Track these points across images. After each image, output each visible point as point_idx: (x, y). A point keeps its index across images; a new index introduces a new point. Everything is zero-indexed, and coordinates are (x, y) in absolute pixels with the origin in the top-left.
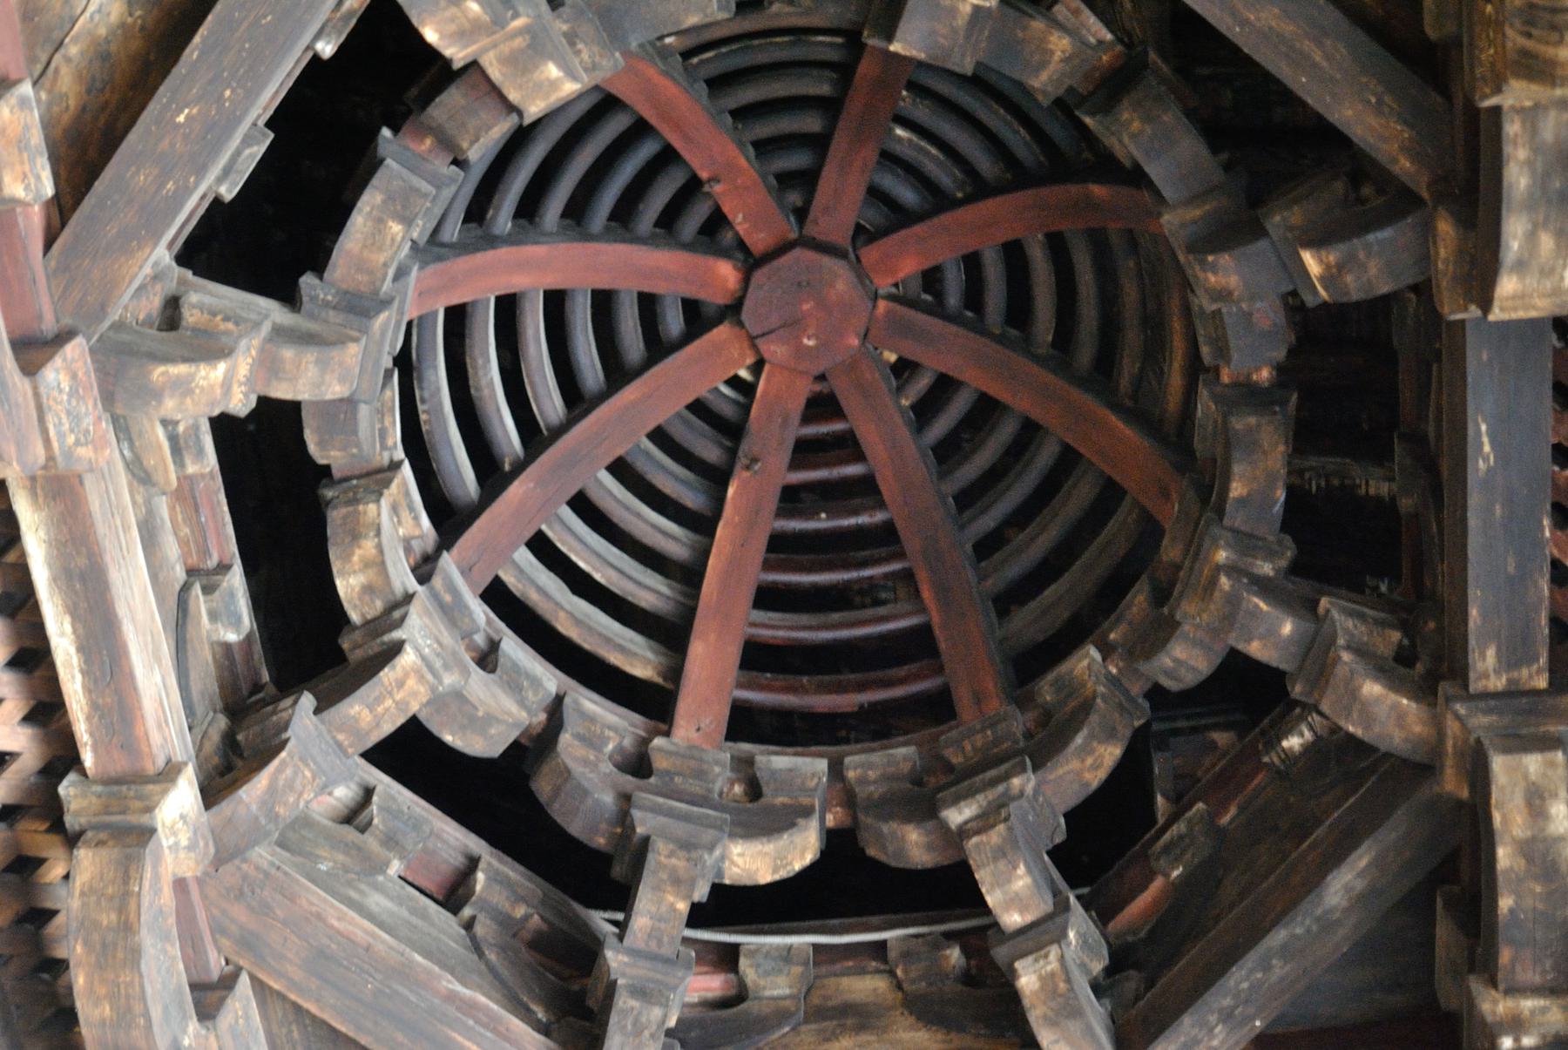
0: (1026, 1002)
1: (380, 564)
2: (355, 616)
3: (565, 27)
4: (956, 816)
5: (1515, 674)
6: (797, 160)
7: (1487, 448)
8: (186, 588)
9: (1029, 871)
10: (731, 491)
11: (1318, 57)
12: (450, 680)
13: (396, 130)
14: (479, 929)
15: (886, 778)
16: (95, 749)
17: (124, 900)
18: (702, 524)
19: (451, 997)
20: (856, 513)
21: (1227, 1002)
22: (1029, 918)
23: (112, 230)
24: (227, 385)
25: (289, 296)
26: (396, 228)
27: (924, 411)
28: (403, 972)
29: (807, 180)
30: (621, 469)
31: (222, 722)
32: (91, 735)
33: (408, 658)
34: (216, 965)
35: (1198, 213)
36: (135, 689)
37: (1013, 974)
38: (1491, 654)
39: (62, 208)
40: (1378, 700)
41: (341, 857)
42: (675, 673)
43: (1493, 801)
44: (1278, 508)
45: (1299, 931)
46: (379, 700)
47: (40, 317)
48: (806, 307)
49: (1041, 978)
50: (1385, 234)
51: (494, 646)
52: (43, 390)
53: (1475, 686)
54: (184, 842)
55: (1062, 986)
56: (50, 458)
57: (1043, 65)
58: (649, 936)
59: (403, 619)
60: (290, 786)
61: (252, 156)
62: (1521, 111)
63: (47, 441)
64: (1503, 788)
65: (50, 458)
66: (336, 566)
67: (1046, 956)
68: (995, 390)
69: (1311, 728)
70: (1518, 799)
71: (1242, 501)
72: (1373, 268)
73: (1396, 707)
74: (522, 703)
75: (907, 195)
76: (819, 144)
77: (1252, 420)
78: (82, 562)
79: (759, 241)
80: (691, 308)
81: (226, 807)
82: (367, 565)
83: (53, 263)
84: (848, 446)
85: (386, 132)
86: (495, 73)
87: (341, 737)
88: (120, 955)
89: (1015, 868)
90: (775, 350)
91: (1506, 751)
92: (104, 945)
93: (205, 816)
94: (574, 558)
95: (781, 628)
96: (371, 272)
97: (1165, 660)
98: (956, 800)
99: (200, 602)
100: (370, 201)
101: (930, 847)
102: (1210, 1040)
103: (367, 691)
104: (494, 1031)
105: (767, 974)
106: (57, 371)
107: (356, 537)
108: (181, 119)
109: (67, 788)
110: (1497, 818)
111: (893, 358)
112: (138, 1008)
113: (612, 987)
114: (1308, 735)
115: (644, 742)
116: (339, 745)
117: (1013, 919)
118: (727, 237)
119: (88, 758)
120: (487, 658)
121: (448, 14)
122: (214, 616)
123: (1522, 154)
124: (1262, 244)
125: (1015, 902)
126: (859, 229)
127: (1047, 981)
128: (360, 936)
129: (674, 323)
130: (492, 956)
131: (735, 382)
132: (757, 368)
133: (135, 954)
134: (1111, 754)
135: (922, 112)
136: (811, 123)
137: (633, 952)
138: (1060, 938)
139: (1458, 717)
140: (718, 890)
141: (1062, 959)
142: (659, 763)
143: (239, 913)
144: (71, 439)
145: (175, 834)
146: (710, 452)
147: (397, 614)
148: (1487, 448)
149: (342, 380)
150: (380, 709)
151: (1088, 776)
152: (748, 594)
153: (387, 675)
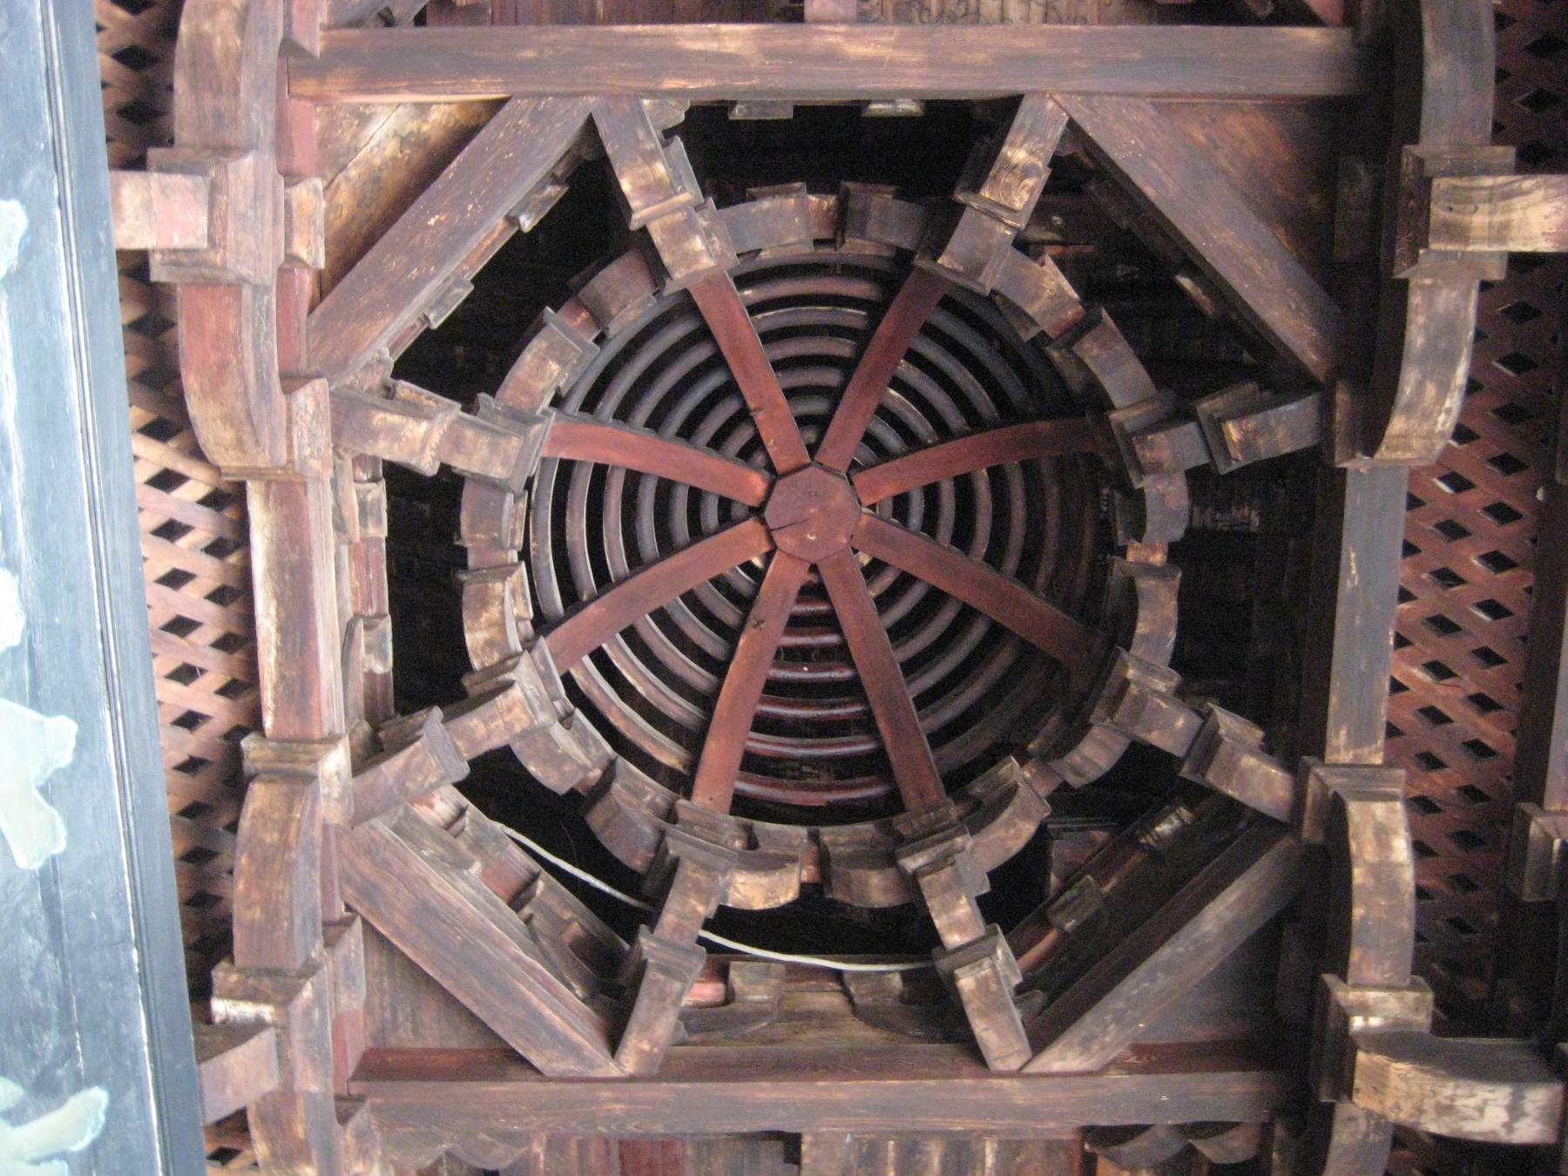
0: (965, 998)
1: (502, 625)
2: (476, 664)
3: (705, 224)
4: (911, 864)
5: (1359, 751)
6: (817, 406)
7: (1354, 572)
9: (969, 903)
10: (742, 642)
11: (1258, 268)
12: (543, 717)
13: (556, 309)
14: (535, 923)
15: (850, 843)
16: (276, 715)
18: (718, 668)
19: (517, 959)
20: (830, 669)
21: (1120, 1005)
22: (966, 939)
23: (364, 301)
24: (425, 441)
25: (469, 405)
26: (554, 367)
27: (884, 602)
28: (486, 934)
29: (820, 423)
30: (662, 618)
32: (275, 701)
33: (516, 692)
34: (340, 911)
35: (1136, 413)
36: (318, 667)
37: (952, 979)
38: (1343, 732)
39: (327, 283)
40: (1253, 770)
41: (440, 849)
42: (693, 765)
43: (1350, 833)
44: (1170, 645)
45: (1180, 950)
46: (493, 718)
47: (298, 359)
48: (812, 511)
49: (977, 980)
50: (1291, 407)
51: (570, 714)
52: (294, 408)
53: (1330, 758)
54: (336, 795)
55: (994, 987)
56: (290, 461)
57: (1037, 297)
58: (675, 929)
59: (515, 666)
60: (420, 768)
61: (458, 296)
62: (1423, 287)
63: (290, 447)
64: (1357, 826)
65: (290, 461)
66: (467, 623)
67: (980, 965)
68: (943, 585)
69: (1179, 818)
71: (1146, 638)
72: (1281, 433)
73: (1266, 774)
74: (587, 754)
75: (892, 440)
76: (834, 395)
77: (1153, 582)
78: (294, 557)
79: (781, 463)
80: (725, 504)
81: (369, 776)
82: (491, 625)
83: (313, 322)
84: (829, 622)
85: (548, 309)
86: (657, 238)
87: (459, 743)
88: (277, 867)
89: (959, 898)
90: (785, 541)
92: (265, 859)
93: (352, 782)
94: (624, 673)
95: (767, 745)
96: (532, 395)
97: (1075, 757)
98: (910, 854)
99: (362, 636)
100: (537, 346)
101: (886, 890)
102: (1105, 1036)
103: (485, 710)
104: (547, 989)
105: (752, 983)
106: (307, 396)
107: (484, 604)
108: (432, 222)
109: (248, 743)
110: (1354, 846)
111: (865, 559)
112: (285, 913)
114: (1176, 823)
116: (457, 749)
117: (953, 939)
118: (759, 458)
119: (268, 721)
120: (566, 720)
121: (641, 171)
122: (369, 649)
123: (1421, 320)
124: (1191, 427)
125: (958, 926)
126: (854, 464)
127: (982, 984)
129: (711, 516)
131: (748, 567)
132: (768, 557)
133: (289, 867)
134: (1028, 829)
135: (913, 375)
136: (831, 378)
137: (659, 941)
138: (991, 953)
139: (1319, 779)
140: (722, 910)
141: (993, 966)
142: (683, 815)
143: (365, 865)
144: (307, 451)
145: (329, 785)
146: (728, 613)
147: (510, 663)
148: (1354, 572)
149: (503, 464)
150: (492, 726)
151: (1010, 843)
152: (748, 721)
153: (500, 700)
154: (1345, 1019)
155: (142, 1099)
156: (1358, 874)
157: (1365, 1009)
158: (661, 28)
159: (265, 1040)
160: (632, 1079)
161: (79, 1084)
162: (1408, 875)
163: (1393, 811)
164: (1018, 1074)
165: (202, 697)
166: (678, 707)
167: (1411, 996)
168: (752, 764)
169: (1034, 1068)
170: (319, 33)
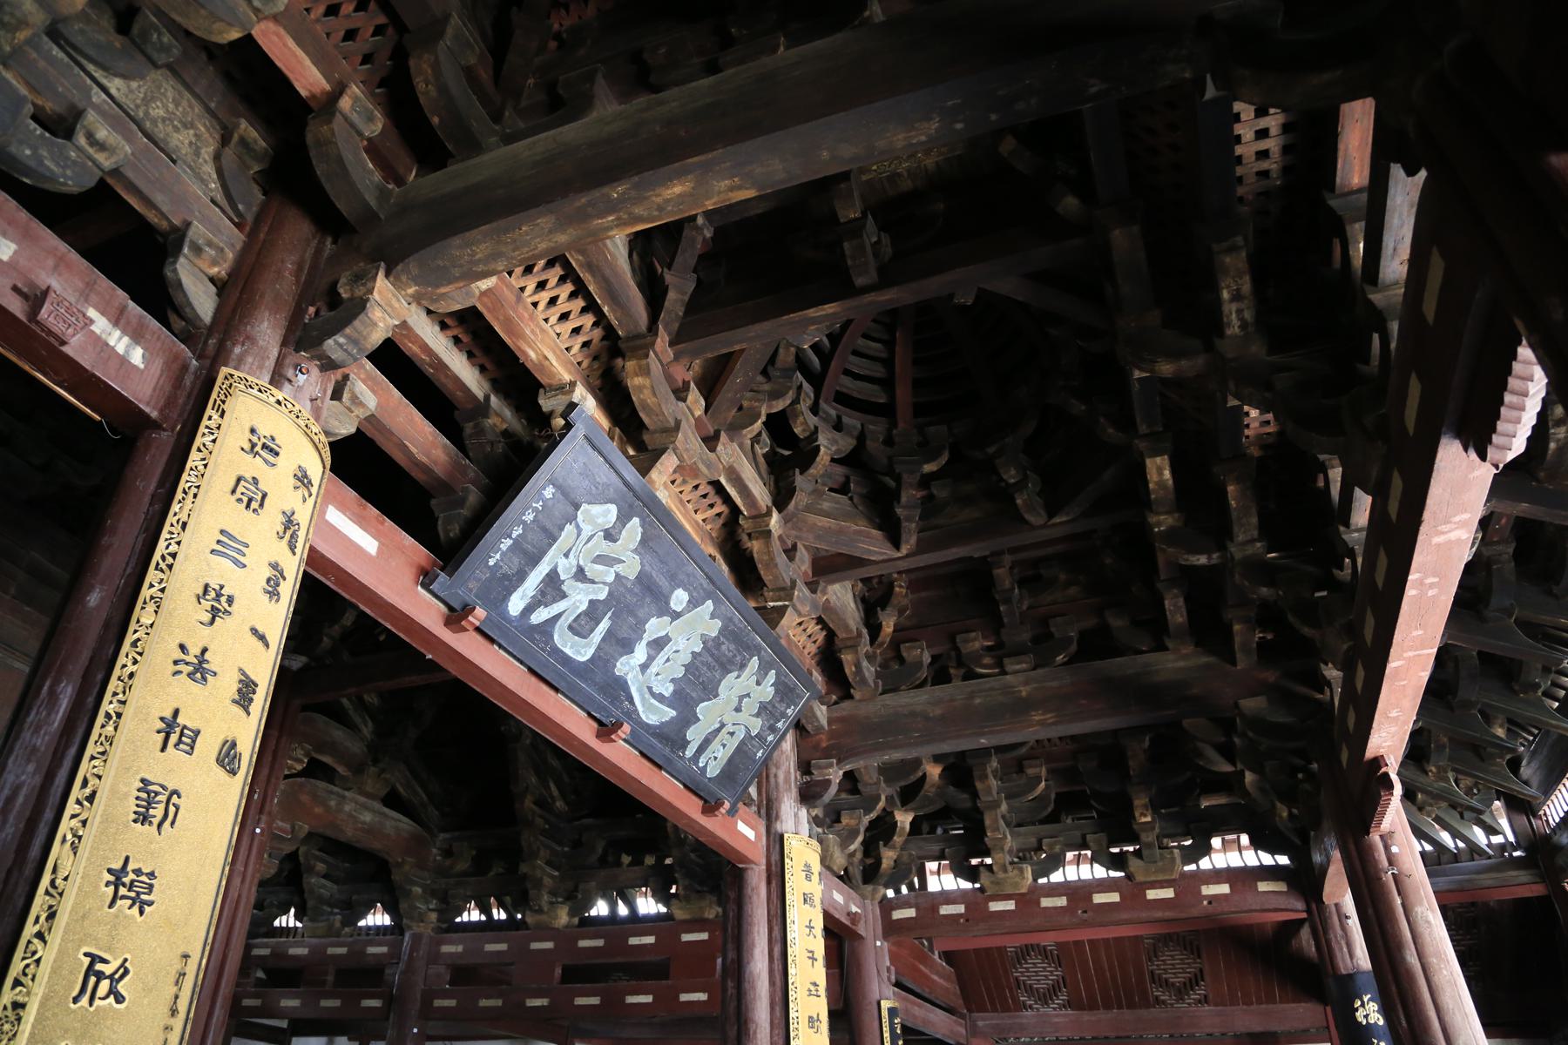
4: (991, 450)
8: (752, 446)
10: (897, 335)
14: (855, 500)
17: (769, 553)
31: (772, 477)
33: (822, 449)
37: (1013, 500)
38: (1144, 427)
42: (892, 397)
70: (1154, 471)
81: (785, 512)
82: (802, 424)
91: (1150, 457)
103: (815, 465)
107: (796, 417)
113: (899, 518)
115: (889, 431)
128: (827, 525)
130: (860, 508)
133: (776, 565)
137: (903, 507)
138: (1027, 486)
142: (897, 439)
153: (818, 459)
154: (1152, 530)
155: (766, 651)
156: (1151, 486)
157: (1159, 524)
158: (800, 313)
159: (790, 610)
160: (907, 556)
161: (749, 660)
162: (1171, 482)
163: (1164, 460)
164: (1044, 526)
165: (720, 508)
166: (878, 371)
167: (1176, 515)
168: (917, 384)
169: (1049, 523)
170: (669, 350)
